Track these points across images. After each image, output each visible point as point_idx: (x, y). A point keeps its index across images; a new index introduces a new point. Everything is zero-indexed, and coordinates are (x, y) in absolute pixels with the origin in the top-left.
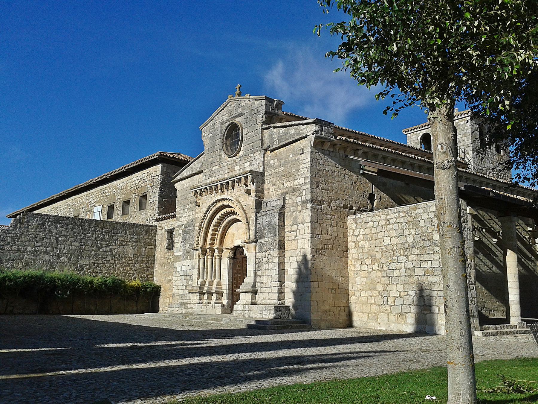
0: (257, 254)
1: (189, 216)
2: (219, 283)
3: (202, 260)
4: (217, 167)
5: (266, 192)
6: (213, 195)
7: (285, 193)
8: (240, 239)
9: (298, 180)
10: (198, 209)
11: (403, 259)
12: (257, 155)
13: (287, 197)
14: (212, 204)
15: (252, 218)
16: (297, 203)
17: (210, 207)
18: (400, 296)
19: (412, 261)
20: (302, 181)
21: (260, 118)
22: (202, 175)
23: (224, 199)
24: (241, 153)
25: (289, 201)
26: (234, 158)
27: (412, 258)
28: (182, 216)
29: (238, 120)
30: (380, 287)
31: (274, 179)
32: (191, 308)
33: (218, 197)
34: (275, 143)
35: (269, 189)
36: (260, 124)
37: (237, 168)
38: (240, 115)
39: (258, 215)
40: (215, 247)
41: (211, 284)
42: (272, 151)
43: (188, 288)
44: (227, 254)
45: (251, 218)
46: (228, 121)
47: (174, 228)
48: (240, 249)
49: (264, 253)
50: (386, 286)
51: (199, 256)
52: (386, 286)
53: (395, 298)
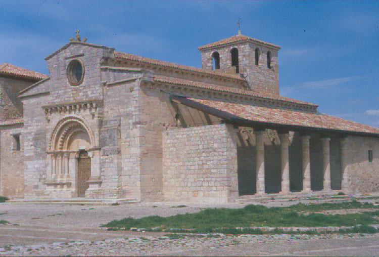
1: (37, 126)
3: (54, 160)
5: (105, 114)
7: (120, 116)
9: (130, 108)
11: (197, 159)
13: (122, 119)
16: (129, 123)
18: (195, 181)
19: (202, 160)
20: (133, 109)
24: (84, 84)
25: (123, 122)
27: (202, 158)
28: (31, 126)
29: (80, 59)
30: (183, 176)
33: (67, 115)
35: (108, 112)
38: (82, 55)
39: (102, 129)
42: (110, 85)
43: (42, 181)
45: (96, 132)
46: (70, 57)
47: (21, 134)
49: (107, 157)
50: (186, 176)
52: (186, 176)
53: (192, 182)
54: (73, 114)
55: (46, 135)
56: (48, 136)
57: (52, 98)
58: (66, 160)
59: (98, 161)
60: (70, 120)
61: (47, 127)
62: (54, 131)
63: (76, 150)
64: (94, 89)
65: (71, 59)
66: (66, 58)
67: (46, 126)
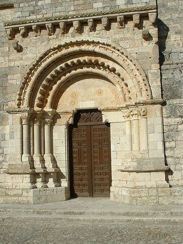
0: (165, 120)
2: (54, 160)
3: (25, 127)
6: (54, 36)
8: (93, 99)
10: (15, 55)
14: (54, 49)
15: (155, 67)
17: (49, 51)
32: (15, 195)
33: (67, 39)
40: (48, 109)
41: (43, 161)
45: (151, 71)
48: (95, 114)
51: (21, 122)
54: (84, 37)
55: (7, 80)
56: (16, 80)
57: (19, 14)
58: (47, 127)
59: (159, 128)
60: (76, 48)
61: (12, 64)
62: (31, 70)
63: (72, 108)
67: (10, 61)
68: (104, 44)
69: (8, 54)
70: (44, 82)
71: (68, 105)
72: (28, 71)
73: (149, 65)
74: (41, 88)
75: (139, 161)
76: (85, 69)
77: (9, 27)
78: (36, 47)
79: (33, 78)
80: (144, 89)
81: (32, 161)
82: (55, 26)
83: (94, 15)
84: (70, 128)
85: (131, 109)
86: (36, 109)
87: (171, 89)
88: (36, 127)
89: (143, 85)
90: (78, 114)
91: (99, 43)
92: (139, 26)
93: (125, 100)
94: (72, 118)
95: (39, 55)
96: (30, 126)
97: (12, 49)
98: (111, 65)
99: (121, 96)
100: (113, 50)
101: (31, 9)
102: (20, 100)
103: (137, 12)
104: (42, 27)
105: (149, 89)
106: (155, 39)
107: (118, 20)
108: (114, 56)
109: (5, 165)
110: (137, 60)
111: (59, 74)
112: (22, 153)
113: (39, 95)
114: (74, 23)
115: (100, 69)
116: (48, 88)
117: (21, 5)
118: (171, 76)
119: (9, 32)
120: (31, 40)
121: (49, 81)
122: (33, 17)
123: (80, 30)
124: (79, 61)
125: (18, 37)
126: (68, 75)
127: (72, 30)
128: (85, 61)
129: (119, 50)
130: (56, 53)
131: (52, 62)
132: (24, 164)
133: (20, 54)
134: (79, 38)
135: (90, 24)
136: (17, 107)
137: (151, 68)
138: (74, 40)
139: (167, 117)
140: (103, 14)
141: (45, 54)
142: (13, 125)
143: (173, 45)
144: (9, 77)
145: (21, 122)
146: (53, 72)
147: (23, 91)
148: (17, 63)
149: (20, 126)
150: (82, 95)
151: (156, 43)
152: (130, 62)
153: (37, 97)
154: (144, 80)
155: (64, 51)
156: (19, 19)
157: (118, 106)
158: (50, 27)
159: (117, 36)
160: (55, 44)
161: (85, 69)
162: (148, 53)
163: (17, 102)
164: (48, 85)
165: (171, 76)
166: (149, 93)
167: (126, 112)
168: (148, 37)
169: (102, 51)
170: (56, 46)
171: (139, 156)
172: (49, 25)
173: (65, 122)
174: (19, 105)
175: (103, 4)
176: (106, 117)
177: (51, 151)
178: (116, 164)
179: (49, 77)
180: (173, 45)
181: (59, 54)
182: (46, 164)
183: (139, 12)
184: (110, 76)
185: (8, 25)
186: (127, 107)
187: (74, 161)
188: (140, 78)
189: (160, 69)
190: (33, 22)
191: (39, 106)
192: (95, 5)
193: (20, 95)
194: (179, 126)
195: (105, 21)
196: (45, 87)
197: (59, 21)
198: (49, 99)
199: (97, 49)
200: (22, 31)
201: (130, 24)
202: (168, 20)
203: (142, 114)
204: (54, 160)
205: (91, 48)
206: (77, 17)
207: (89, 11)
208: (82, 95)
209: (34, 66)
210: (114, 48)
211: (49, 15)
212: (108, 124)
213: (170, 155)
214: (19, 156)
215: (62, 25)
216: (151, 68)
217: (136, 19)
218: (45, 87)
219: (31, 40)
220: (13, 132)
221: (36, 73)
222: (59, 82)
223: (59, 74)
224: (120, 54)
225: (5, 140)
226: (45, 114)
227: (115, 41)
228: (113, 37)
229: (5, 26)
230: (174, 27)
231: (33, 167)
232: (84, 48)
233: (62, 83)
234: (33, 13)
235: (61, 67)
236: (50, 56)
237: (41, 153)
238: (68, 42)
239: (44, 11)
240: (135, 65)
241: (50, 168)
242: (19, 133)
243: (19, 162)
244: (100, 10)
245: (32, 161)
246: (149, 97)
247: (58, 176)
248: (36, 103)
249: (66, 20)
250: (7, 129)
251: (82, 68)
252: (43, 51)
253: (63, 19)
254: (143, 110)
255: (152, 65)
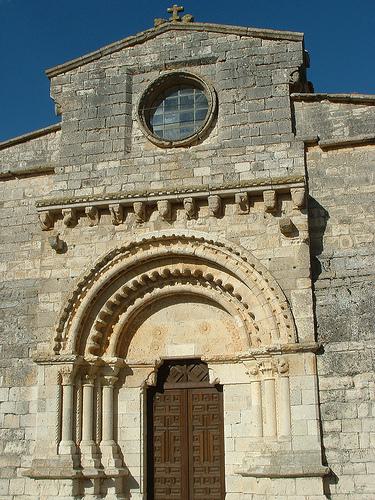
2: (118, 453)
3: (67, 390)
4: (117, 164)
6: (123, 226)
8: (192, 341)
10: (53, 258)
12: (279, 151)
14: (123, 250)
15: (303, 285)
17: (114, 253)
21: (284, 76)
22: (42, 181)
23: (174, 240)
26: (183, 150)
29: (195, 70)
31: (344, 208)
34: (337, 133)
36: (286, 87)
37: (203, 171)
40: (109, 357)
41: (97, 454)
42: (326, 148)
44: (143, 377)
46: (155, 68)
48: (197, 368)
49: (346, 380)
51: (60, 380)
54: (178, 228)
55: (37, 303)
56: (52, 304)
58: (106, 391)
59: (310, 396)
60: (162, 249)
62: (81, 286)
63: (154, 357)
64: (266, 156)
65: (155, 76)
66: (131, 73)
67: (43, 268)
68: (211, 242)
69: (41, 255)
70: (104, 309)
71: (147, 350)
72: (76, 288)
73: (293, 281)
74: (98, 319)
75: (275, 457)
76: (178, 287)
77: (44, 208)
78: (90, 245)
79: (84, 302)
80: (283, 324)
81: (77, 454)
82: (126, 209)
83: (194, 192)
84: (151, 393)
85: (259, 361)
86: (89, 357)
87: (332, 324)
88: (87, 390)
89: (281, 317)
90: (165, 368)
91: (202, 240)
92: (275, 210)
93: (250, 344)
94: (153, 375)
95: (97, 260)
96: (76, 388)
97: (48, 247)
98: (226, 279)
99: (244, 336)
100: (228, 253)
101: (85, 176)
102: (58, 339)
103: (270, 187)
104: (102, 210)
105: (292, 325)
106: (304, 234)
107: (237, 200)
108: (230, 264)
109: (27, 462)
110: (270, 272)
111: (131, 296)
112: (60, 439)
113: (93, 332)
114: (160, 204)
115: (205, 286)
116: (110, 319)
117: (68, 170)
118: (332, 300)
119: (43, 218)
120: (81, 233)
121: (113, 306)
122: (87, 191)
123: (170, 217)
124: (167, 272)
125: (60, 226)
126: (147, 296)
127: (155, 216)
128: (177, 271)
129: (238, 254)
130: (127, 256)
131: (120, 273)
132: (62, 459)
133: (61, 258)
134: (169, 231)
135: (188, 206)
136: (53, 352)
137: (296, 287)
138: (158, 235)
139: (326, 376)
140: (211, 190)
141: (107, 259)
142: (45, 387)
143: (336, 242)
144: (41, 297)
145: (60, 380)
146: (120, 291)
147: (66, 323)
148: (56, 273)
149: (57, 388)
150: (172, 333)
151: (305, 241)
152: (257, 275)
153: (90, 336)
154: (283, 308)
155: (141, 254)
156: (62, 195)
157: (237, 354)
158: (116, 210)
159: (237, 229)
160: (124, 240)
161: (178, 287)
162: (290, 259)
163: (54, 343)
164: (110, 313)
165: (332, 300)
166: (293, 332)
167: (253, 365)
168: (290, 231)
169: (209, 255)
170: (126, 245)
171: (275, 448)
172: (115, 206)
173: (140, 382)
174: (57, 349)
175: (212, 169)
176: (216, 373)
177: (114, 437)
178: (233, 461)
179: (112, 299)
180: (336, 242)
181: (132, 259)
182: (104, 461)
183: (274, 187)
184: (224, 299)
185: (43, 206)
186: (253, 356)
187: (157, 454)
188: (277, 305)
189: (313, 288)
190: (88, 201)
191: (94, 351)
192: (198, 172)
193: (60, 331)
194: (347, 391)
195: (213, 201)
196: (105, 317)
197: (133, 200)
198: (112, 339)
199: (200, 251)
200: (67, 217)
201: (259, 208)
202: (326, 198)
203: (280, 369)
204: (118, 453)
205: (188, 249)
206: (165, 194)
207: (188, 183)
208: (172, 333)
209: (87, 279)
210: (230, 250)
211: (113, 190)
212: (219, 387)
213: (331, 445)
214: (55, 444)
215: (137, 207)
216: (296, 287)
217: (269, 197)
218: (105, 317)
219: (81, 233)
220: (44, 400)
221: (90, 292)
222: (130, 308)
223: (131, 296)
224: (241, 261)
225: (28, 413)
226: (103, 367)
227: (233, 238)
228: (229, 230)
229: (38, 206)
230: (337, 212)
231: (78, 466)
232: (176, 248)
233: (136, 310)
234: (88, 183)
235: (135, 283)
236: (116, 262)
237: (94, 439)
238: (148, 237)
239: (107, 181)
240: (267, 281)
241: (110, 466)
242: (55, 401)
243: (53, 455)
244: (207, 181)
245: (77, 454)
246: (293, 340)
247: (126, 483)
248: (88, 346)
249: (144, 199)
250: (34, 393)
251: (172, 284)
252: (103, 253)
253: (140, 197)
254: (282, 362)
255: (298, 281)
